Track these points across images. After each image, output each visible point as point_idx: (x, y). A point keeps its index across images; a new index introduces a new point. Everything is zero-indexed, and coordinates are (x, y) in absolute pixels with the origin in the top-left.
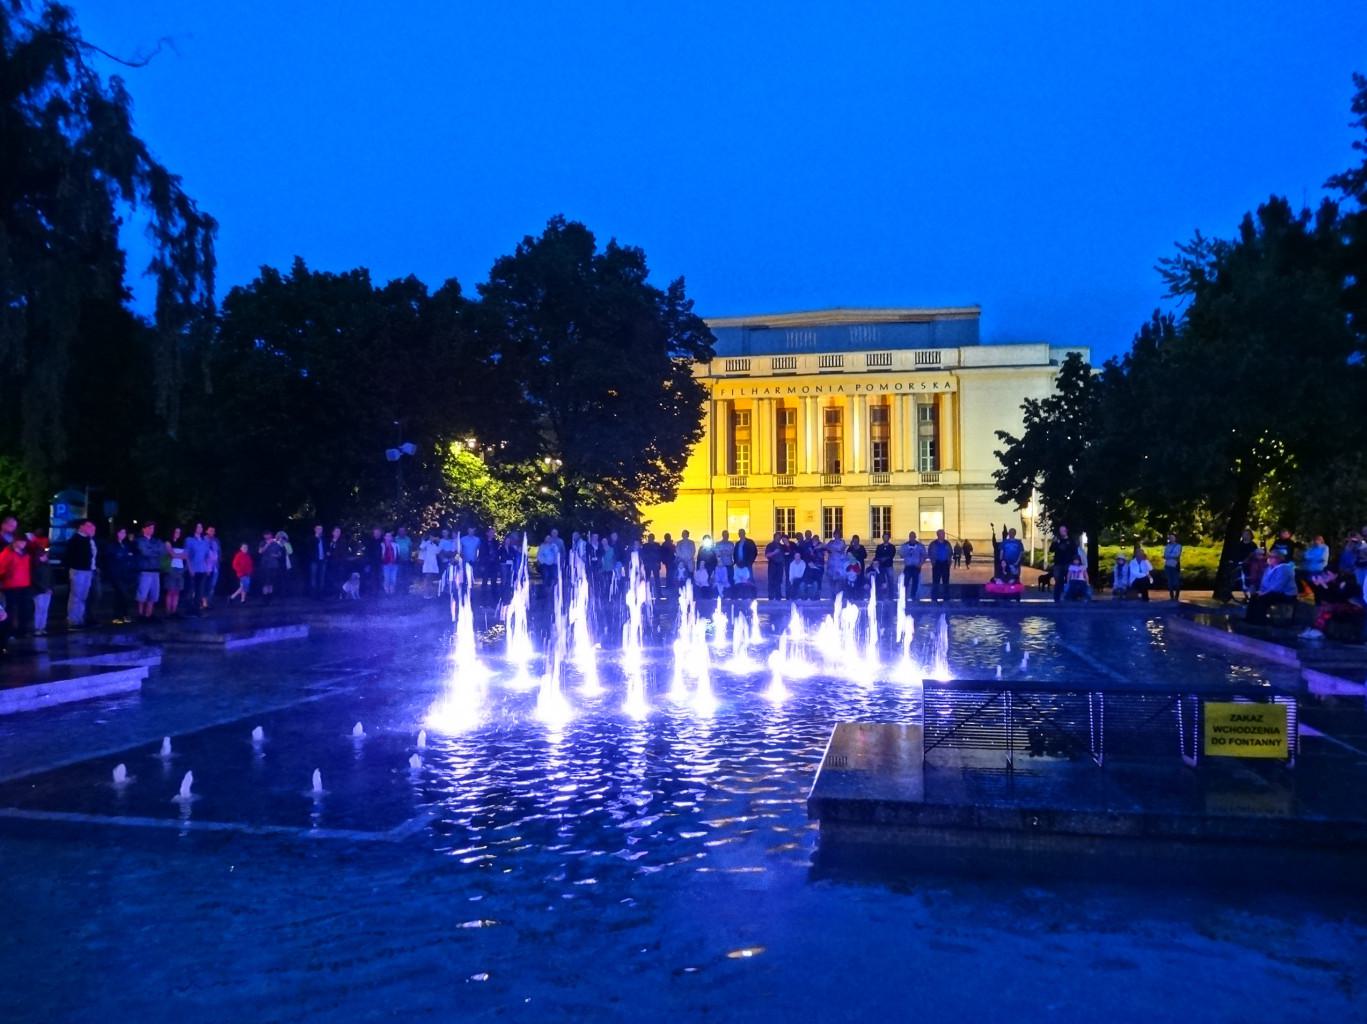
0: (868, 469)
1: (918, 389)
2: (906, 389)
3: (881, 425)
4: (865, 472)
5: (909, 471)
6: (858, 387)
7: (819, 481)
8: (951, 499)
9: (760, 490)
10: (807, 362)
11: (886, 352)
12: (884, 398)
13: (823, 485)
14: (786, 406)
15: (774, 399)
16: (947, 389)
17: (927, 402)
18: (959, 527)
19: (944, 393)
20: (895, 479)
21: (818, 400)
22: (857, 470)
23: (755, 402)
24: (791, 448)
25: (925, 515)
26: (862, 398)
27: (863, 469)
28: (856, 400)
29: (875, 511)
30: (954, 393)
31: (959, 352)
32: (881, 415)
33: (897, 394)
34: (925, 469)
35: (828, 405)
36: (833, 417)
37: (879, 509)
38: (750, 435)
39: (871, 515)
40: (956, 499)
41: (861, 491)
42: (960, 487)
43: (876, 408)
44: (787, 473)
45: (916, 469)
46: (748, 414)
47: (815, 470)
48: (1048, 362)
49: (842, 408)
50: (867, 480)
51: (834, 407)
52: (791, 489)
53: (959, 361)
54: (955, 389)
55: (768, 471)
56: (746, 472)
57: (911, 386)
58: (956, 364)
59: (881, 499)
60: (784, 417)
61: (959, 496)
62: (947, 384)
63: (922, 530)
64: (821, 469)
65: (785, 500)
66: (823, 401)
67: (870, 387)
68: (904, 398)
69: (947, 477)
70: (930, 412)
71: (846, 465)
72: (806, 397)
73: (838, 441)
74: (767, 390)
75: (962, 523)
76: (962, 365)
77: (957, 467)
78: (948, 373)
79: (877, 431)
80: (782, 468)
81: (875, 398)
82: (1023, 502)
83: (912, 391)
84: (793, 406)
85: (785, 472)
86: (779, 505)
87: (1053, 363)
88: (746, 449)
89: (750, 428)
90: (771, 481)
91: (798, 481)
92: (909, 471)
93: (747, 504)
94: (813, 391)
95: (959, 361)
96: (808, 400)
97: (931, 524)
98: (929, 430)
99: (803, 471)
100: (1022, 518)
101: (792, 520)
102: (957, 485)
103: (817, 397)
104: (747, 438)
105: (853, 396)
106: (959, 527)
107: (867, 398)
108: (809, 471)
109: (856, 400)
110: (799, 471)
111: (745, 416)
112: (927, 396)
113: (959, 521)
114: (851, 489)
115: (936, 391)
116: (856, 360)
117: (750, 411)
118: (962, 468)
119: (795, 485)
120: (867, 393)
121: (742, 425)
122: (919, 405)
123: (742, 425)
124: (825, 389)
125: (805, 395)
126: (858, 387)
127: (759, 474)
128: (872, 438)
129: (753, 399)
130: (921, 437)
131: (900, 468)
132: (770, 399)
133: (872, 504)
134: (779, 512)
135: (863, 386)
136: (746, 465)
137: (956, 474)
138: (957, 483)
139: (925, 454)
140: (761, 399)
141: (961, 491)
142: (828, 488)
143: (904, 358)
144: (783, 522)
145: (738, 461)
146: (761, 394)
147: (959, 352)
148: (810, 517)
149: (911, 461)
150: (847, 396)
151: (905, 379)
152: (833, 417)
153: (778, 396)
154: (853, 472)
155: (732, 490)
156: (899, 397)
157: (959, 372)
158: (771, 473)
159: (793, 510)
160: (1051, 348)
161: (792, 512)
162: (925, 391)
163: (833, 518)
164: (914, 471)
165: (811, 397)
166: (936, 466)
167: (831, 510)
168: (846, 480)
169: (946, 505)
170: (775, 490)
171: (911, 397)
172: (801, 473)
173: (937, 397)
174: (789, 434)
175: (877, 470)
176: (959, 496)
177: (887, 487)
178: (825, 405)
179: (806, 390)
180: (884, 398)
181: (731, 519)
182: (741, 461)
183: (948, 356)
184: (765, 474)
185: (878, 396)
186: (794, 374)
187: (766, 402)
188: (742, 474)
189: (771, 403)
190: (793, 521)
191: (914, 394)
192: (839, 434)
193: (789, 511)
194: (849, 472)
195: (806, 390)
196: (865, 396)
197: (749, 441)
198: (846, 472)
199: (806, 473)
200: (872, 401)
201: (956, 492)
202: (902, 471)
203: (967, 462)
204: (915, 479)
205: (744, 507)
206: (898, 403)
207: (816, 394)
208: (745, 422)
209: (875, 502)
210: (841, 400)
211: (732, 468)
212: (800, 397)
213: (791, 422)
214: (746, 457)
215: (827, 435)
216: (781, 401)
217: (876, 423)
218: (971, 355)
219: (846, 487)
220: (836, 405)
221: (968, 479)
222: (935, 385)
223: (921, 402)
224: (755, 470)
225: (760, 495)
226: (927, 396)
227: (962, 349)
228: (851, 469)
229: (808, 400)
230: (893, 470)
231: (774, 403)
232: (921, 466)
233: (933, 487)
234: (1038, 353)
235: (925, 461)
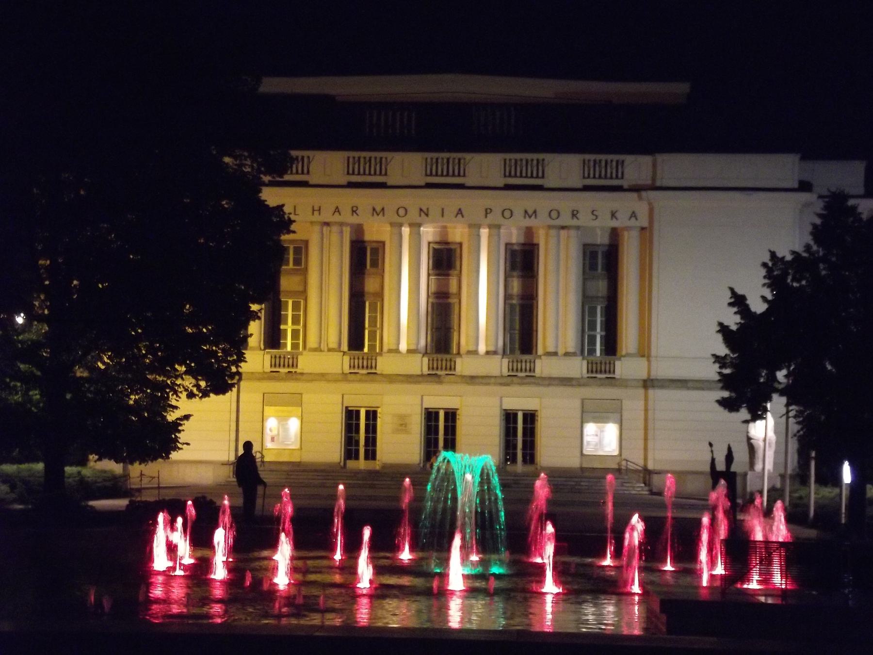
0: (500, 350)
1: (585, 219)
2: (566, 219)
3: (522, 277)
4: (495, 353)
5: (567, 354)
6: (488, 212)
7: (419, 365)
8: (633, 403)
9: (322, 377)
10: (407, 165)
11: (535, 156)
12: (529, 232)
13: (426, 371)
14: (368, 237)
15: (347, 224)
16: (633, 222)
17: (599, 241)
18: (646, 449)
19: (628, 229)
20: (543, 367)
21: (422, 229)
22: (482, 348)
23: (317, 228)
24: (373, 309)
25: (590, 429)
26: (495, 231)
27: (492, 348)
28: (484, 232)
29: (509, 417)
30: (643, 229)
31: (654, 165)
32: (522, 261)
33: (550, 227)
34: (592, 351)
35: (438, 239)
36: (445, 260)
37: (515, 415)
38: (305, 283)
39: (503, 423)
40: (642, 403)
41: (488, 384)
42: (648, 383)
43: (516, 247)
44: (366, 350)
45: (578, 352)
46: (302, 249)
47: (413, 347)
48: (796, 186)
49: (461, 244)
50: (499, 366)
51: (447, 243)
52: (373, 375)
53: (654, 179)
54: (644, 222)
55: (333, 343)
56: (295, 346)
57: (574, 214)
58: (649, 182)
59: (520, 400)
60: (364, 258)
61: (646, 399)
62: (634, 215)
63: (585, 452)
64: (423, 343)
65: (362, 396)
66: (429, 232)
67: (507, 214)
68: (563, 233)
69: (625, 368)
70: (603, 262)
71: (463, 339)
72: (401, 225)
73: (451, 301)
74: (337, 210)
75: (650, 444)
76: (658, 184)
77: (644, 352)
78: (634, 195)
79: (516, 286)
80: (356, 341)
81: (515, 232)
82: (757, 413)
83: (575, 222)
84: (381, 239)
85: (361, 347)
86: (352, 402)
87: (805, 186)
88: (296, 306)
89: (305, 272)
90: (338, 363)
91: (385, 365)
92: (567, 354)
93: (296, 400)
94: (413, 215)
95: (654, 179)
96: (406, 230)
97: (603, 439)
98: (601, 287)
99: (393, 347)
100: (749, 439)
101: (372, 429)
102: (645, 381)
103: (419, 225)
104: (301, 288)
105: (479, 227)
106: (646, 449)
107: (503, 231)
108: (403, 347)
109: (484, 232)
110: (385, 349)
111: (298, 251)
112: (599, 232)
113: (646, 439)
114: (472, 379)
115: (614, 224)
116: (485, 166)
117: (306, 242)
118: (654, 352)
119: (378, 371)
120: (501, 220)
121: (291, 265)
122: (585, 246)
123: (291, 265)
124: (435, 212)
125: (400, 220)
126: (488, 212)
127: (318, 350)
128: (507, 297)
129: (312, 223)
130: (587, 301)
131: (551, 349)
132: (342, 224)
133: (505, 407)
134: (351, 415)
135: (497, 211)
136: (295, 334)
137: (643, 362)
138: (645, 376)
139: (592, 327)
140: (327, 224)
141: (651, 392)
142: (432, 377)
143: (564, 167)
144: (357, 431)
145: (282, 327)
146: (327, 216)
147: (654, 165)
148: (402, 425)
149: (570, 339)
150: (470, 226)
151: (565, 203)
152: (445, 260)
153: (354, 220)
154: (475, 352)
155: (273, 376)
156: (553, 232)
157: (652, 194)
158: (338, 349)
159: (375, 413)
160: (803, 158)
161: (372, 415)
162: (596, 223)
163: (441, 430)
164: (574, 354)
165: (411, 225)
166: (611, 347)
167: (437, 414)
168: (463, 366)
169: (625, 413)
170: (344, 377)
171: (573, 233)
172: (390, 351)
173: (615, 234)
174: (370, 285)
175: (512, 351)
176: (646, 399)
177: (532, 378)
178: (431, 239)
179: (402, 212)
180: (529, 232)
181: (272, 424)
182: (288, 327)
183: (636, 167)
184: (329, 350)
185: (519, 228)
186: (383, 186)
187: (335, 229)
188: (289, 348)
189: (342, 232)
190: (375, 431)
191: (578, 228)
192: (453, 289)
193: (367, 412)
194: (469, 352)
195: (402, 212)
196: (498, 227)
197: (303, 293)
198: (463, 349)
199: (397, 351)
200: (511, 234)
201: (641, 391)
202: (555, 354)
203: (660, 343)
204: (577, 367)
205: (297, 406)
206: (552, 242)
207: (418, 220)
208: (297, 262)
209: (511, 404)
210: (458, 233)
211: (273, 339)
212: (392, 224)
213: (375, 264)
214: (296, 321)
215: (433, 289)
216: (358, 230)
217: (515, 274)
218: (677, 166)
219: (463, 377)
220: (451, 239)
221: (663, 370)
222: (613, 215)
223: (589, 241)
224: (312, 341)
225: (323, 384)
226: (599, 232)
227: (660, 158)
228: (471, 348)
229: (406, 230)
230: (540, 351)
231: (347, 231)
232: (585, 348)
233: (603, 383)
234: (784, 167)
235: (592, 341)
